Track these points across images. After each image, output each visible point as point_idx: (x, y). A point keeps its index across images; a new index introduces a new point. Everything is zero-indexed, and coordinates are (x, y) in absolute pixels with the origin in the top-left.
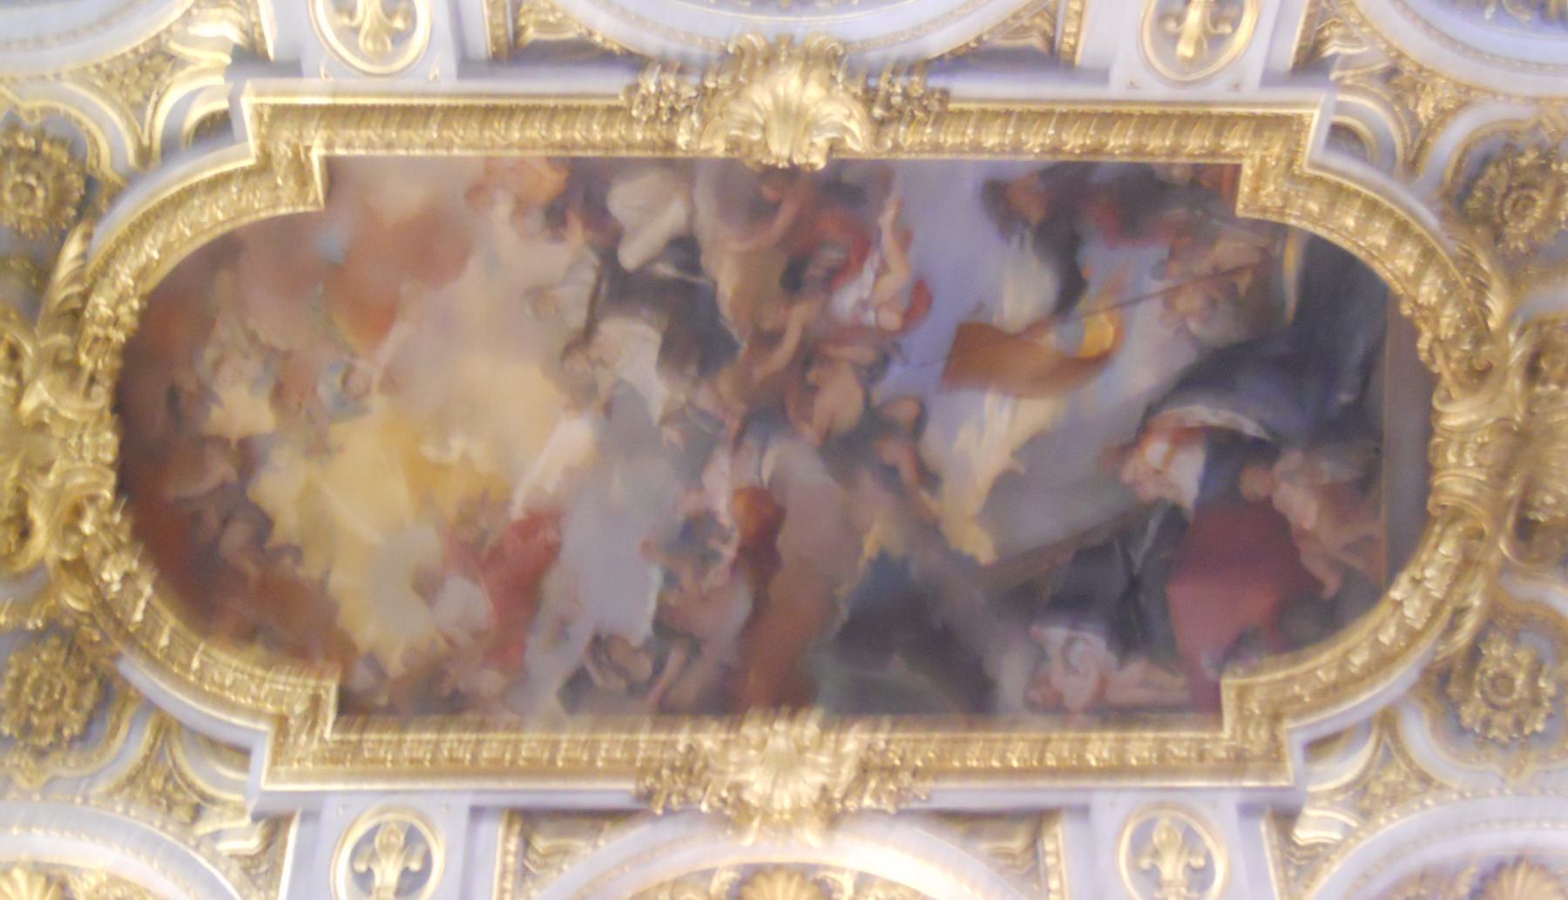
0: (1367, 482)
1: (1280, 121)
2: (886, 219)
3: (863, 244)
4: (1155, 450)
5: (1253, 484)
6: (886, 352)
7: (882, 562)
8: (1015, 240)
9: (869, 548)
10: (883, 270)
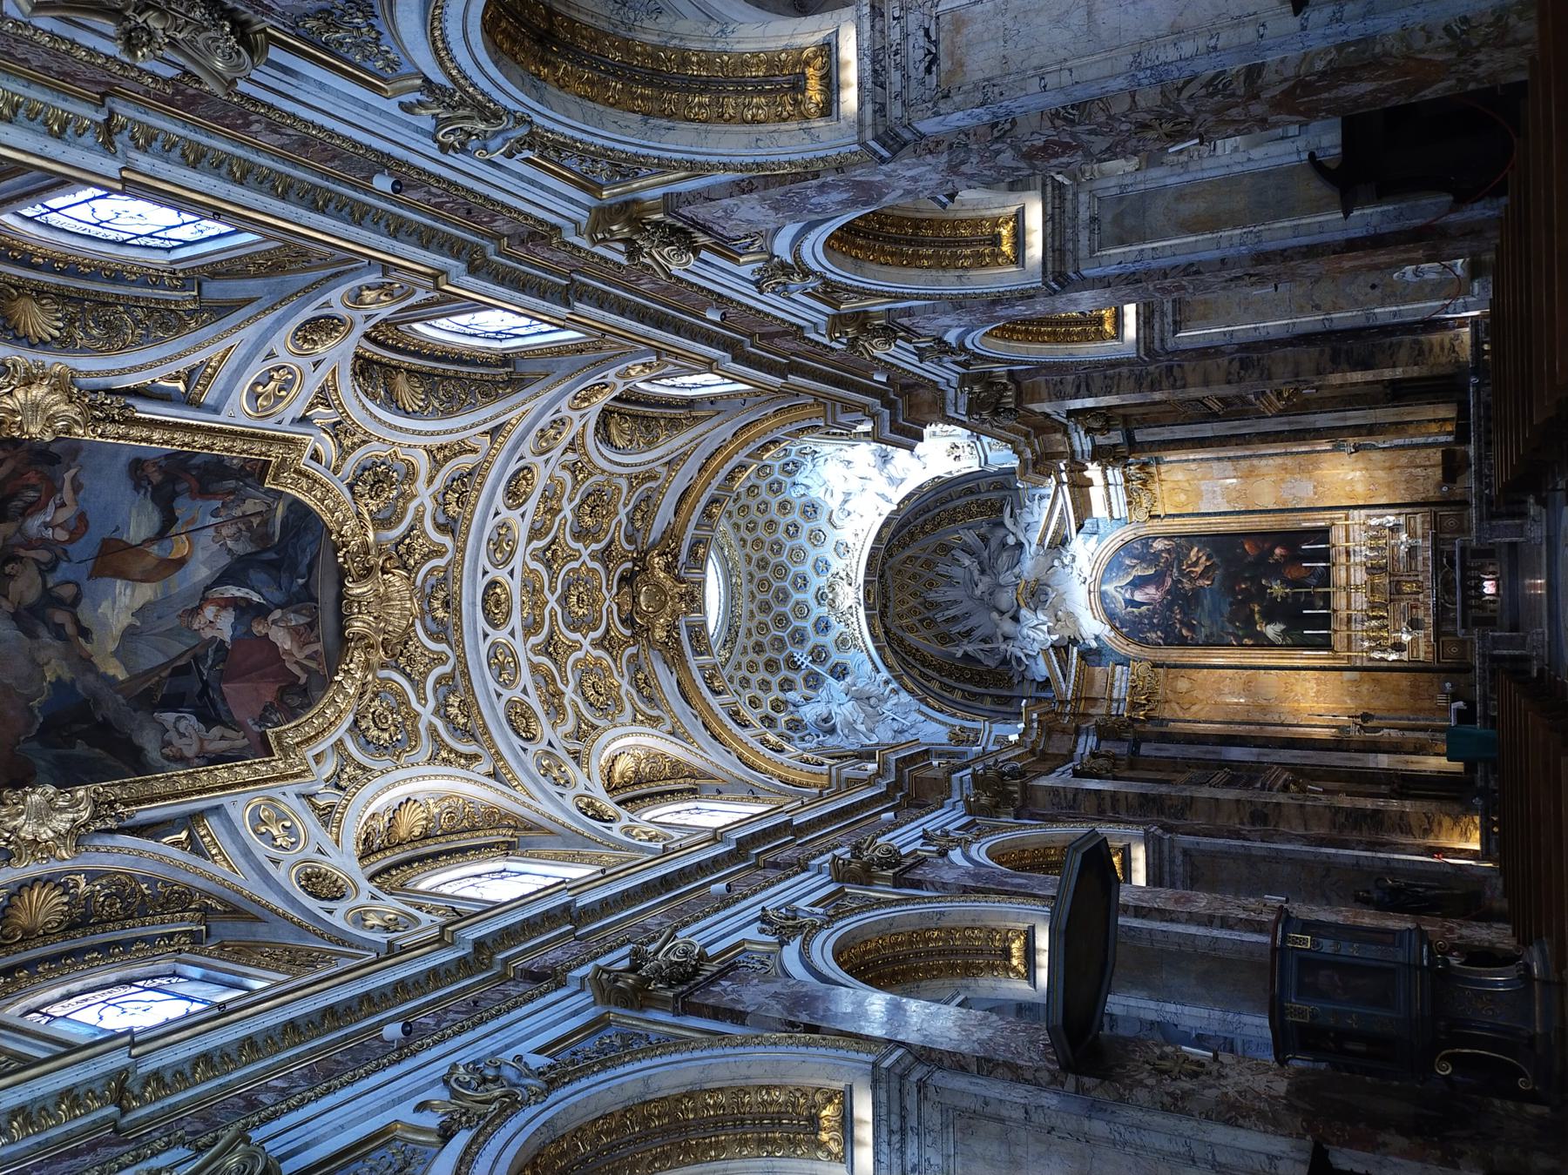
0: (311, 626)
1: (292, 441)
2: (68, 476)
3: (54, 489)
4: (209, 612)
5: (258, 629)
6: (59, 554)
7: (58, 684)
8: (142, 492)
9: (50, 677)
10: (63, 505)
